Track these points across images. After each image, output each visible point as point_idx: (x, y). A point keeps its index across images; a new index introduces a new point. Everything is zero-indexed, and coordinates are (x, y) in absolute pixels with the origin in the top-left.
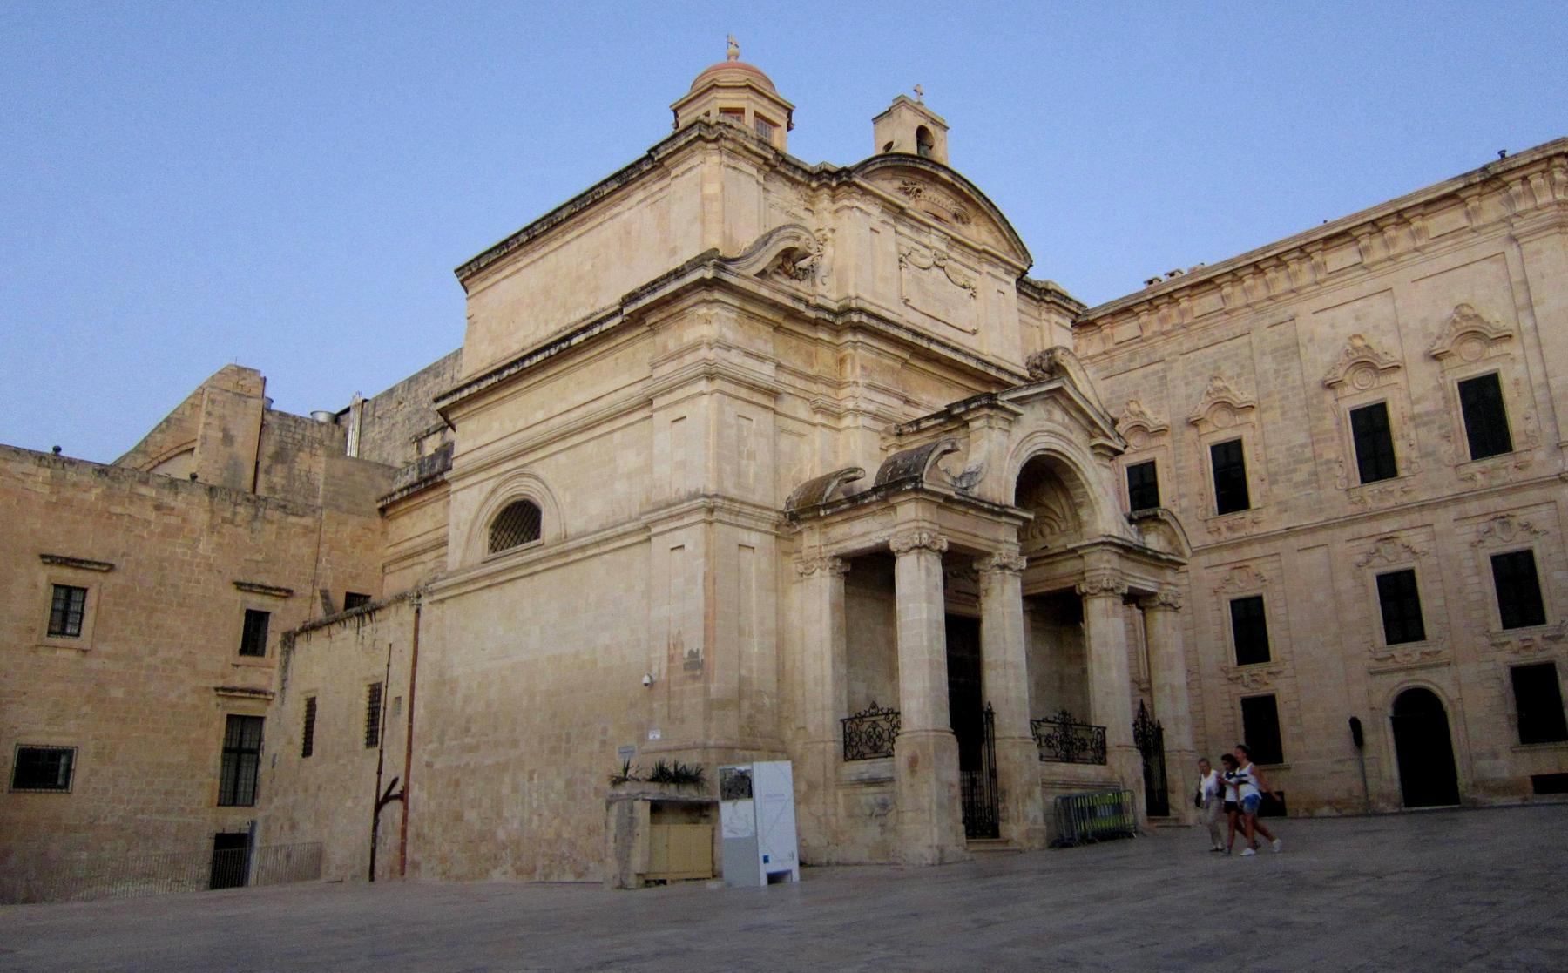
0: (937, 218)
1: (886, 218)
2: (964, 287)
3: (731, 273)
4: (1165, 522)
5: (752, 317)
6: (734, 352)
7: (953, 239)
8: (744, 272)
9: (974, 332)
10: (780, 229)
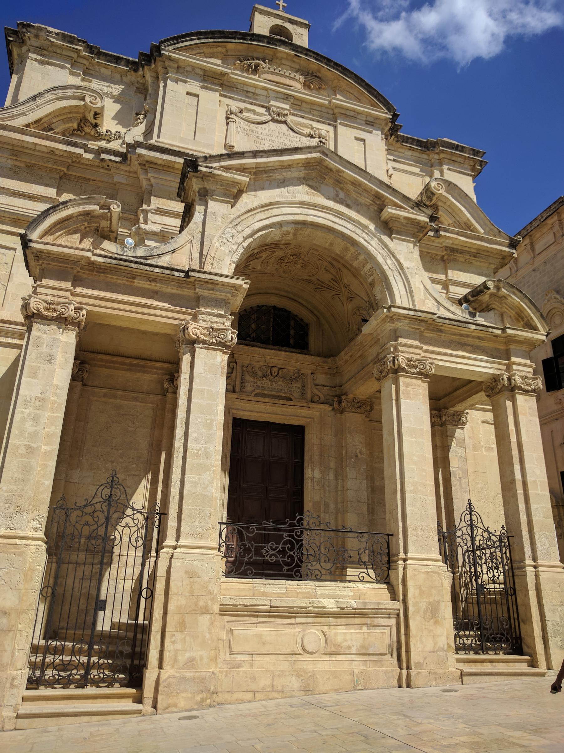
10: (54, 89)
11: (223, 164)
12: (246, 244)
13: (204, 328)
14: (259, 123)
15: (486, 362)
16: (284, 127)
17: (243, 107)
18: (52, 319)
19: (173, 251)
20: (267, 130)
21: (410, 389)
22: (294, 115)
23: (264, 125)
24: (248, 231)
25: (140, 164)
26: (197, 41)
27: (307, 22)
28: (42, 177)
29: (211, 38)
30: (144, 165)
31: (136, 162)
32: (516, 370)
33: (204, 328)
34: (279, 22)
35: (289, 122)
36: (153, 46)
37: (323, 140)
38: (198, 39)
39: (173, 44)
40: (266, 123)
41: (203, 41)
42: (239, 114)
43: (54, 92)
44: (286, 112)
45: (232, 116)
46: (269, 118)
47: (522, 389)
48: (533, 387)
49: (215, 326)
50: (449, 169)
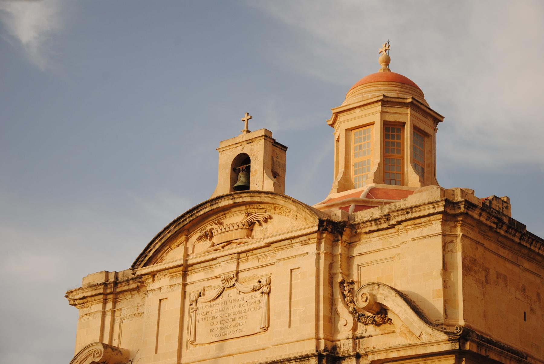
2: (254, 290)
9: (266, 329)
20: (220, 304)
23: (218, 299)
26: (160, 244)
29: (168, 233)
34: (238, 151)
37: (265, 289)
38: (160, 241)
39: (143, 261)
40: (219, 296)
41: (163, 241)
43: (76, 361)
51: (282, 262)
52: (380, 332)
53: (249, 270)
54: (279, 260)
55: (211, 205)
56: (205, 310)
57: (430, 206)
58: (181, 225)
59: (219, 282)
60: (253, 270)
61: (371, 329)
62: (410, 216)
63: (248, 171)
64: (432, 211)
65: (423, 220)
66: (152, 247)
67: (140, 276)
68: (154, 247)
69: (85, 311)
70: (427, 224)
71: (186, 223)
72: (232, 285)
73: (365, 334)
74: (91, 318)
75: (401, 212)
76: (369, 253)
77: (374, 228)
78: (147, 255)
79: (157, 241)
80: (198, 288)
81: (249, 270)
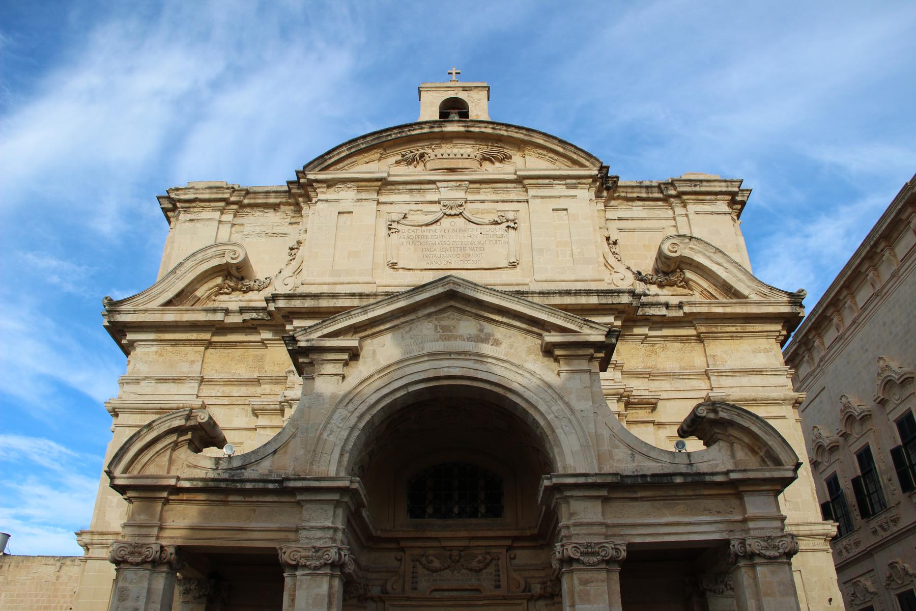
0: (452, 170)
1: (364, 195)
3: (128, 312)
4: (731, 423)
5: (175, 343)
6: (143, 383)
7: (472, 182)
8: (149, 306)
9: (513, 265)
10: (193, 255)
11: (326, 331)
12: (362, 425)
13: (305, 549)
14: (427, 225)
15: (709, 523)
16: (459, 221)
17: (406, 211)
18: (137, 564)
19: (275, 452)
20: (438, 231)
21: (592, 588)
22: (472, 202)
23: (434, 226)
24: (363, 408)
25: (283, 317)
26: (348, 153)
27: (485, 85)
28: (186, 354)
30: (288, 317)
31: (279, 316)
32: (754, 529)
33: (305, 549)
34: (451, 94)
35: (466, 214)
36: (297, 172)
37: (512, 225)
38: (348, 149)
40: (437, 222)
41: (353, 150)
42: (403, 221)
44: (459, 203)
45: (394, 225)
46: (440, 215)
47: (765, 557)
48: (781, 551)
49: (319, 544)
50: (697, 213)
51: (538, 201)
52: (670, 293)
53: (483, 202)
54: (535, 197)
55: (431, 128)
56: (413, 234)
57: (723, 184)
58: (384, 139)
59: (436, 208)
60: (485, 205)
61: (654, 289)
62: (697, 189)
63: (464, 114)
64: (724, 189)
65: (708, 197)
66: (335, 153)
67: (311, 183)
68: (338, 154)
69: (189, 216)
70: (711, 202)
71: (390, 138)
72: (458, 213)
73: (647, 292)
74: (198, 225)
75: (689, 183)
76: (632, 219)
77: (644, 195)
78: (326, 160)
79: (345, 148)
80: (405, 208)
81: (483, 202)
